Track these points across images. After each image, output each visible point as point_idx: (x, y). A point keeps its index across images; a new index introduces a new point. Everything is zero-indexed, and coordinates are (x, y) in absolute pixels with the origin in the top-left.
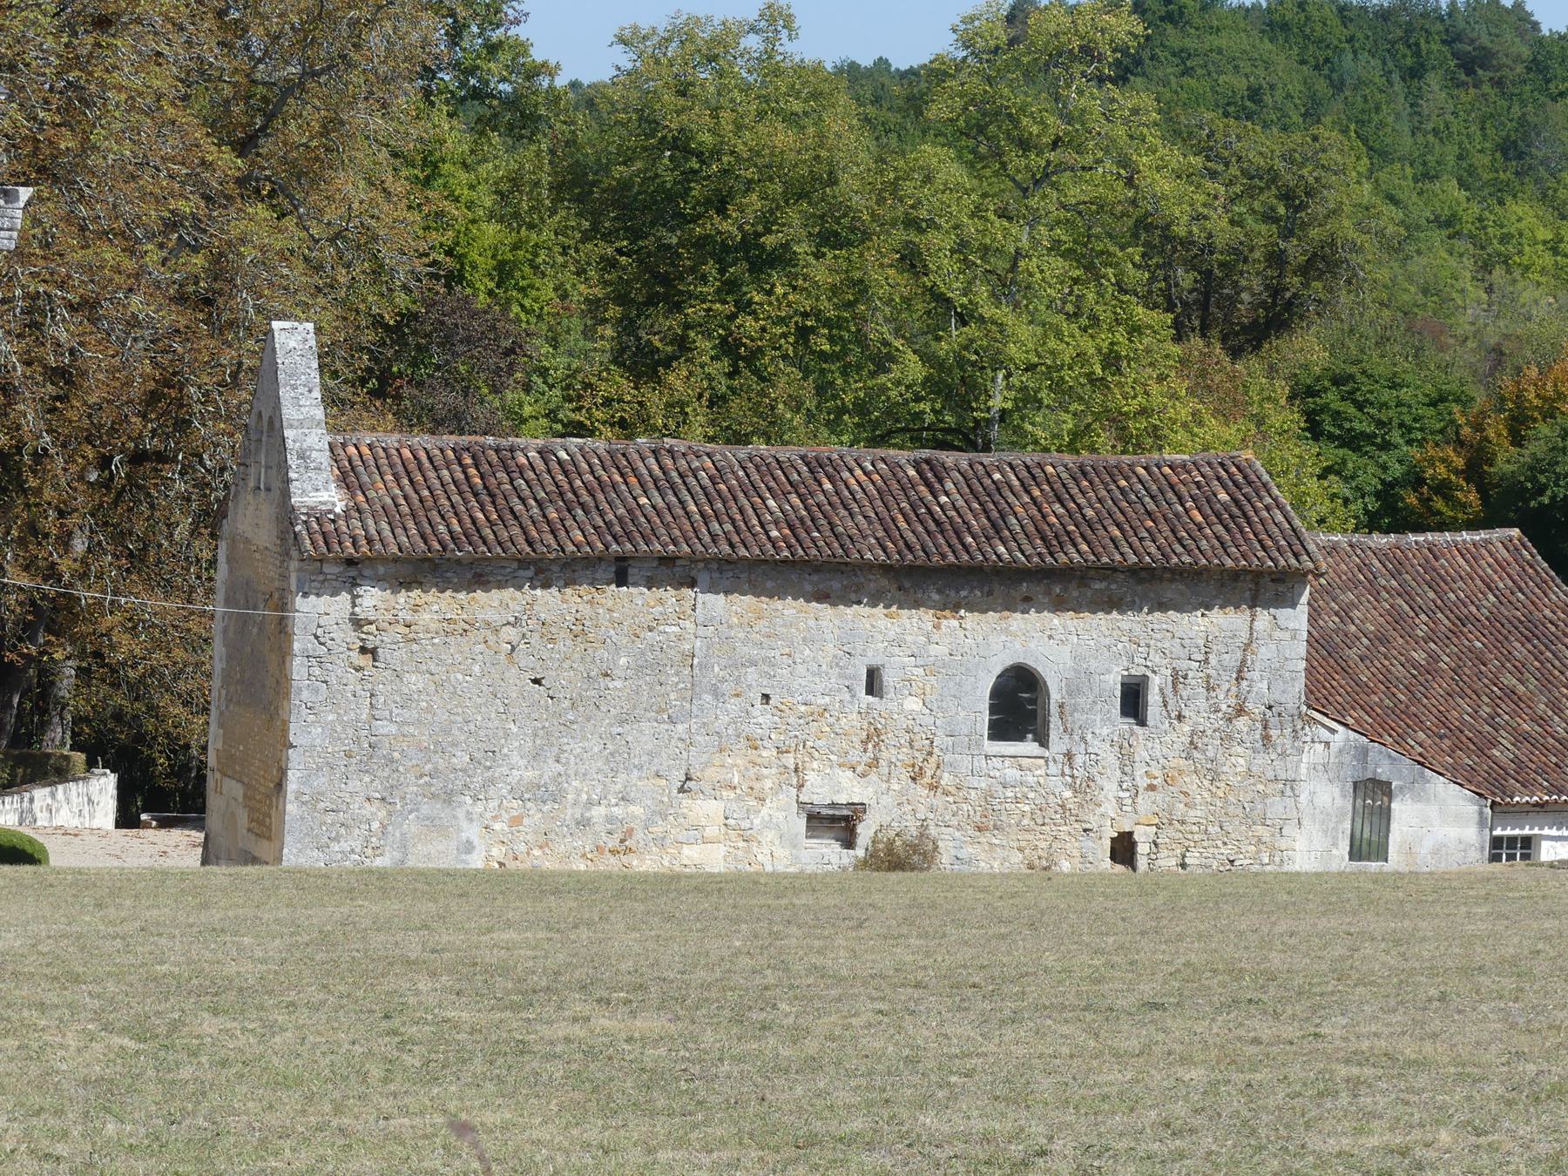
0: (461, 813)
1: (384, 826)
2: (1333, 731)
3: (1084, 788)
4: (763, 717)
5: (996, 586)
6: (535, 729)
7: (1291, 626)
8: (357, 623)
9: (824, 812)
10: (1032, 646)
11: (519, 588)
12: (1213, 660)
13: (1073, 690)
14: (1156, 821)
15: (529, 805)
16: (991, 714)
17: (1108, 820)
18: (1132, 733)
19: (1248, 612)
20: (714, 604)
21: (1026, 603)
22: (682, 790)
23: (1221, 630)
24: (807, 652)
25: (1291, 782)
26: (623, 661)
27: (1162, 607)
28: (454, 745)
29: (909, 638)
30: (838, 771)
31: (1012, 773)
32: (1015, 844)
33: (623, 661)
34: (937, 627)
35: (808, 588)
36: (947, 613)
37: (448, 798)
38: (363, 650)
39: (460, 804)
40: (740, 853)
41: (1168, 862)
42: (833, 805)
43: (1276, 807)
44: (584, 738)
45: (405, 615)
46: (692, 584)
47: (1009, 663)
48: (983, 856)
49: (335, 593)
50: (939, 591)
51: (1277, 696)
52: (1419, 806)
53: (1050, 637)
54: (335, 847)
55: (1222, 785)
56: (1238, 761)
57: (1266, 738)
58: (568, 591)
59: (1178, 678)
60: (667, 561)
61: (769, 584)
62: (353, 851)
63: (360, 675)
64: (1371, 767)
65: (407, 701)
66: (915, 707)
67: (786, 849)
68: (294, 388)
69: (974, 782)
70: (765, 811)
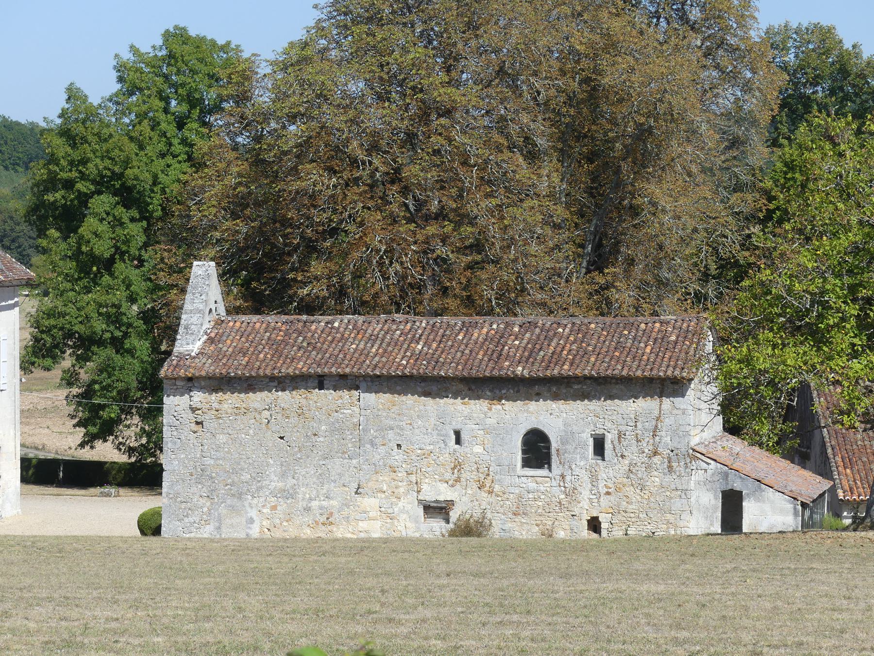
0: (246, 504)
1: (209, 510)
2: (708, 464)
3: (572, 493)
4: (398, 456)
5: (521, 388)
6: (282, 462)
7: (682, 407)
8: (193, 410)
9: (432, 505)
10: (541, 418)
11: (270, 391)
12: (639, 425)
13: (564, 441)
14: (612, 511)
15: (280, 500)
16: (523, 454)
17: (585, 510)
18: (597, 464)
19: (658, 400)
20: (370, 398)
21: (538, 396)
22: (356, 493)
23: (643, 410)
24: (420, 422)
25: (685, 491)
26: (323, 428)
27: (611, 397)
28: (242, 470)
29: (475, 415)
30: (439, 484)
31: (532, 485)
32: (534, 523)
33: (323, 428)
34: (490, 409)
35: (420, 390)
36: (495, 402)
37: (240, 496)
38: (197, 423)
39: (246, 499)
40: (388, 525)
41: (618, 533)
42: (437, 501)
43: (677, 504)
44: (306, 467)
45: (215, 405)
46: (357, 388)
47: (529, 427)
48: (517, 528)
49: (182, 395)
50: (490, 391)
51: (675, 445)
52: (759, 504)
53: (551, 414)
54: (186, 520)
55: (646, 492)
56: (656, 480)
57: (670, 467)
58: (294, 393)
59: (620, 436)
60: (343, 377)
61: (398, 388)
62: (195, 522)
63: (195, 435)
64: (730, 483)
65: (218, 448)
66: (480, 451)
67: (412, 524)
68: (194, 294)
69: (512, 490)
70: (400, 504)
